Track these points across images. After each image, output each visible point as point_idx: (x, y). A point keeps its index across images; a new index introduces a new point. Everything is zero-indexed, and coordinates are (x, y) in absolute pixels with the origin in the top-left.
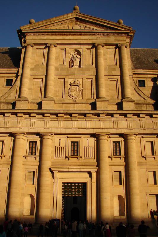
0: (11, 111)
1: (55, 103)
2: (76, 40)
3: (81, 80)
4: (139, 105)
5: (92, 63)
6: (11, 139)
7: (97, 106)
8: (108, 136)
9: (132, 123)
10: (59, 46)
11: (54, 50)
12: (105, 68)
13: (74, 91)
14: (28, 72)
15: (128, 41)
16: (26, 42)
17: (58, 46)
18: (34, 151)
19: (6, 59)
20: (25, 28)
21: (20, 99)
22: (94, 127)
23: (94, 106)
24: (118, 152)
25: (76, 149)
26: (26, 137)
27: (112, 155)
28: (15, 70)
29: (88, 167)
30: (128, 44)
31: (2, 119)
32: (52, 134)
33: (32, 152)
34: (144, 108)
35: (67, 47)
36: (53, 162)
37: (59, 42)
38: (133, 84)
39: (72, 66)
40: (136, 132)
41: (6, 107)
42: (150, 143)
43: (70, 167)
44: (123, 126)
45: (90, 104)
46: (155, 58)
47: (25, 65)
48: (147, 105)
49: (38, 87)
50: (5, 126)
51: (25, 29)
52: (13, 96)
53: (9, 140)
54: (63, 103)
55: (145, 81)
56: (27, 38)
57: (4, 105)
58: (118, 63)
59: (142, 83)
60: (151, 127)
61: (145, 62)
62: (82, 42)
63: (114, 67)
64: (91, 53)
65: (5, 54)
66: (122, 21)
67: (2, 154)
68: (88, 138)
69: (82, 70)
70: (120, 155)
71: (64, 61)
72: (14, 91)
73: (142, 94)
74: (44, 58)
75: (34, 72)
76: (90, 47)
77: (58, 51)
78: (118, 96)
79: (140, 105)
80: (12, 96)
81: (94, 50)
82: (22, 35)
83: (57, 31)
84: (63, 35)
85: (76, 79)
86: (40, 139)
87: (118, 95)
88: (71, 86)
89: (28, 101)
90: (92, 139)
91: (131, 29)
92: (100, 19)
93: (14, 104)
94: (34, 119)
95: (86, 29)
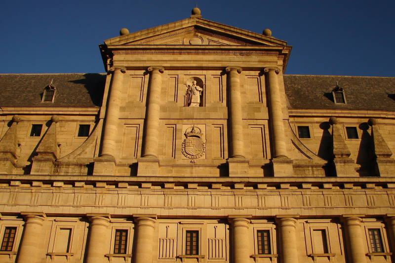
0: (85, 178)
1: (160, 166)
2: (195, 62)
3: (202, 127)
4: (300, 169)
5: (221, 99)
6: (84, 225)
7: (230, 170)
8: (249, 221)
9: (290, 198)
10: (167, 71)
11: (158, 78)
12: (243, 108)
13: (191, 145)
14: (115, 113)
15: (281, 62)
16: (114, 65)
17: (166, 72)
18: (123, 247)
19: (80, 91)
20: (112, 42)
21: (100, 158)
22: (225, 205)
23: (224, 170)
24: (266, 247)
25: (194, 244)
26: (110, 222)
27: (257, 253)
28: (93, 110)
30: (281, 68)
31: (71, 191)
32: (155, 218)
33: (120, 249)
35: (179, 72)
37: (168, 65)
38: (290, 133)
39: (189, 105)
40: (296, 214)
41: (77, 170)
42: (320, 232)
44: (273, 203)
45: (219, 167)
46: (325, 90)
47: (111, 102)
48: (314, 168)
49: (132, 139)
50: (75, 204)
51: (113, 44)
52: (89, 153)
53: (80, 228)
54: (173, 166)
55: (310, 128)
56: (115, 57)
57: (74, 168)
58: (265, 99)
59: (304, 132)
60: (322, 205)
61: (308, 96)
62: (205, 65)
63: (258, 106)
64: (221, 83)
65: (78, 85)
66: (269, 32)
67: (68, 252)
68: (214, 225)
69: (205, 111)
70: (270, 253)
71: (176, 96)
72: (92, 145)
73: (304, 150)
74: (142, 90)
75: (126, 114)
76: (219, 72)
77: (166, 79)
78: (265, 153)
79: (302, 169)
81: (225, 77)
82: (107, 53)
83: (165, 47)
84: (173, 53)
85: (196, 125)
86: (133, 226)
88: (187, 138)
89: (115, 162)
90: (223, 225)
91: (285, 44)
92: (234, 28)
93: (91, 167)
95: (213, 43)
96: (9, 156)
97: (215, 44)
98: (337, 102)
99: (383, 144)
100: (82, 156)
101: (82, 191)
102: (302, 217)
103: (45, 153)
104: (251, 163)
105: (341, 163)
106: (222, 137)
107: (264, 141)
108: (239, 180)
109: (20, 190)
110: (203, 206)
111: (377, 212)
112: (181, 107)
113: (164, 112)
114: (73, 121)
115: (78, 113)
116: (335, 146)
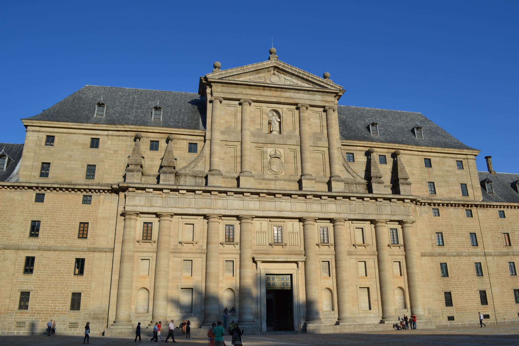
0: (204, 188)
3: (282, 150)
14: (218, 136)
17: (253, 104)
29: (293, 256)
36: (254, 250)
37: (255, 98)
38: (341, 158)
39: (271, 132)
43: (275, 256)
44: (332, 209)
47: (215, 126)
52: (202, 167)
54: (263, 179)
57: (190, 179)
58: (325, 131)
59: (351, 157)
62: (282, 100)
69: (283, 138)
72: (202, 161)
73: (351, 172)
82: (204, 85)
83: (253, 84)
87: (324, 171)
94: (231, 198)
96: (139, 167)
97: (288, 83)
100: (195, 169)
101: (201, 197)
102: (349, 220)
103: (169, 167)
104: (317, 180)
108: (310, 193)
109: (153, 195)
110: (285, 210)
111: (396, 218)
112: (266, 134)
114: (184, 139)
115: (187, 133)
116: (372, 171)
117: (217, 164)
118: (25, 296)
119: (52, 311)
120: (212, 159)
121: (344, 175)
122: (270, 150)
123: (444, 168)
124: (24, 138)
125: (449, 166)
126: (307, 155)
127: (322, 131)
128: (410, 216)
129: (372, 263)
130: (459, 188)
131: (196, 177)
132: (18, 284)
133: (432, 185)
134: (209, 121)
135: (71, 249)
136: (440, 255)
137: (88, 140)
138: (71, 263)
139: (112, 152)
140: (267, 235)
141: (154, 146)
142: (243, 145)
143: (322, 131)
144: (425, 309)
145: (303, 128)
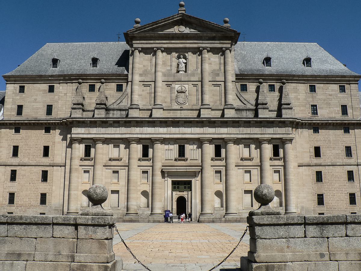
1: (164, 110)
7: (201, 113)
12: (209, 74)
34: (244, 113)
36: (163, 163)
37: (166, 46)
38: (235, 89)
39: (178, 72)
41: (119, 112)
43: (178, 168)
47: (134, 71)
52: (125, 103)
58: (222, 68)
59: (244, 88)
69: (188, 76)
73: (243, 100)
75: (143, 79)
80: (124, 102)
85: (183, 85)
87: (220, 100)
98: (266, 66)
99: (287, 97)
105: (261, 109)
106: (197, 92)
107: (221, 94)
108: (206, 119)
112: (174, 73)
113: (164, 77)
116: (260, 98)
117: (137, 100)
118: (12, 196)
119: (29, 205)
120: (133, 96)
121: (237, 104)
122: (177, 87)
123: (326, 93)
124: (5, 89)
125: (332, 90)
126: (208, 87)
127: (220, 69)
128: (289, 134)
129: (255, 172)
130: (339, 109)
131: (120, 110)
132: (7, 188)
133: (314, 108)
134: (130, 66)
135: (39, 164)
136: (316, 165)
137: (46, 87)
138: (39, 174)
139: (63, 94)
140: (173, 152)
141: (92, 88)
142: (156, 84)
143: (220, 69)
144: (297, 207)
145: (204, 67)
